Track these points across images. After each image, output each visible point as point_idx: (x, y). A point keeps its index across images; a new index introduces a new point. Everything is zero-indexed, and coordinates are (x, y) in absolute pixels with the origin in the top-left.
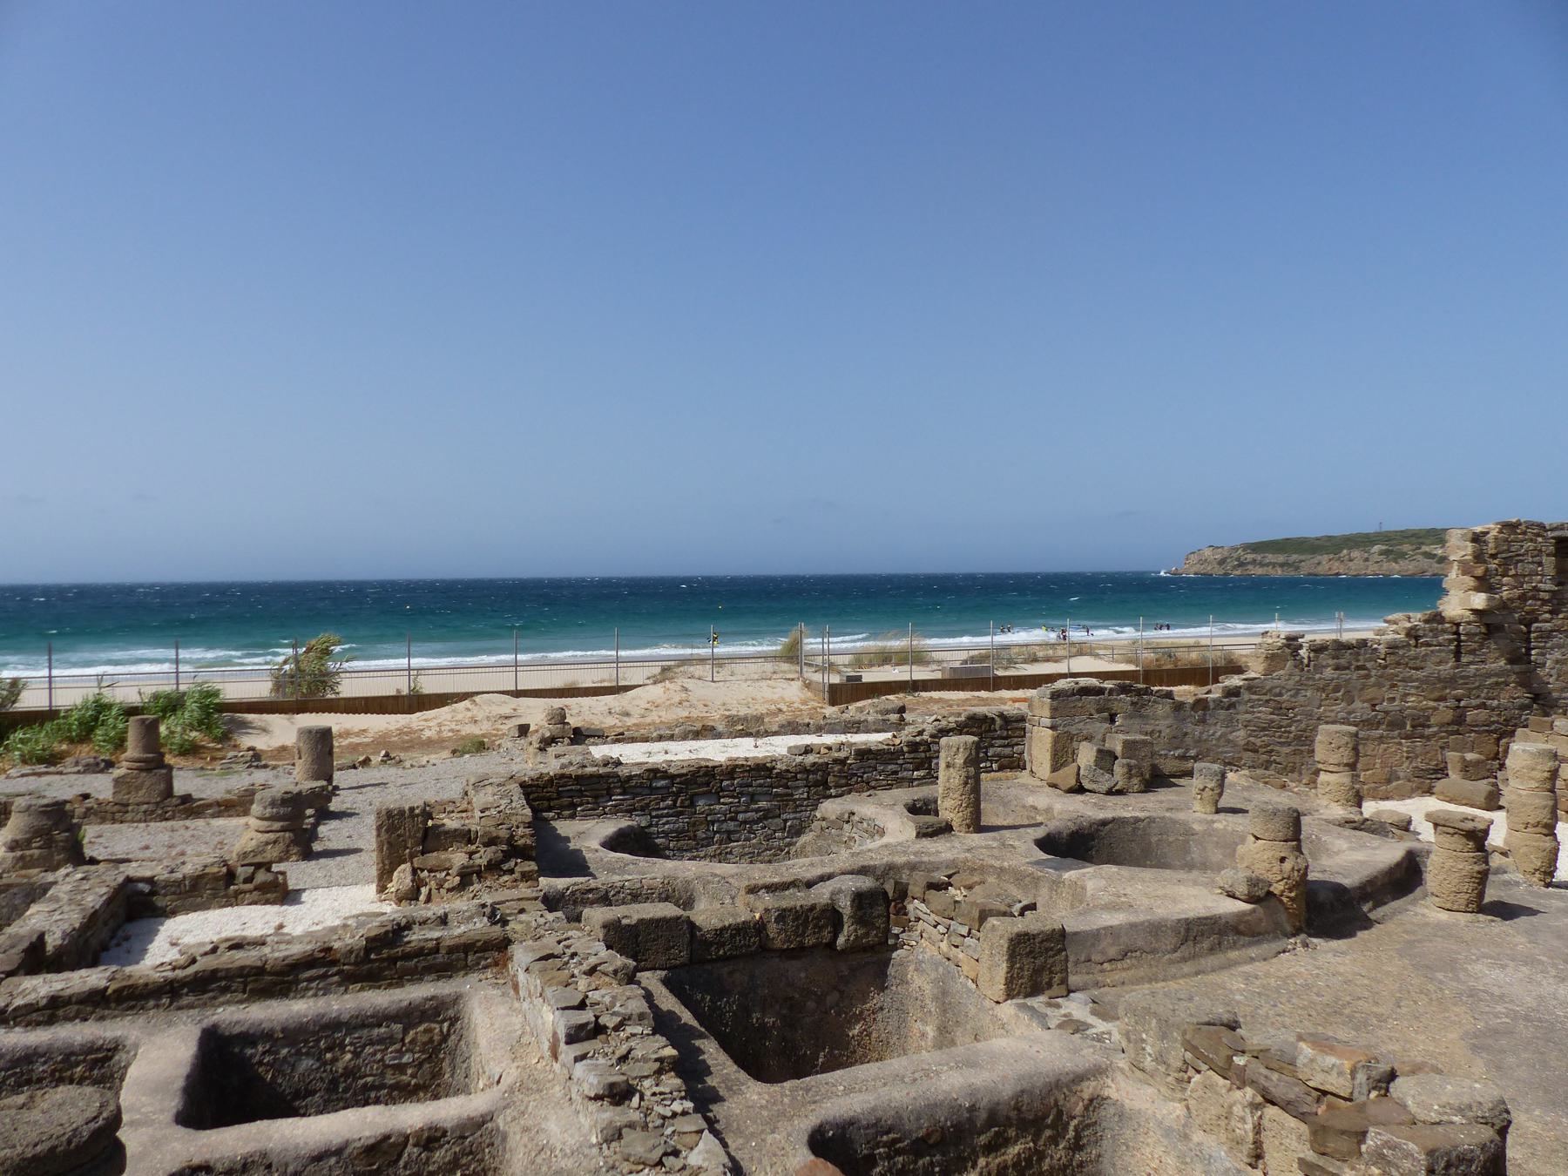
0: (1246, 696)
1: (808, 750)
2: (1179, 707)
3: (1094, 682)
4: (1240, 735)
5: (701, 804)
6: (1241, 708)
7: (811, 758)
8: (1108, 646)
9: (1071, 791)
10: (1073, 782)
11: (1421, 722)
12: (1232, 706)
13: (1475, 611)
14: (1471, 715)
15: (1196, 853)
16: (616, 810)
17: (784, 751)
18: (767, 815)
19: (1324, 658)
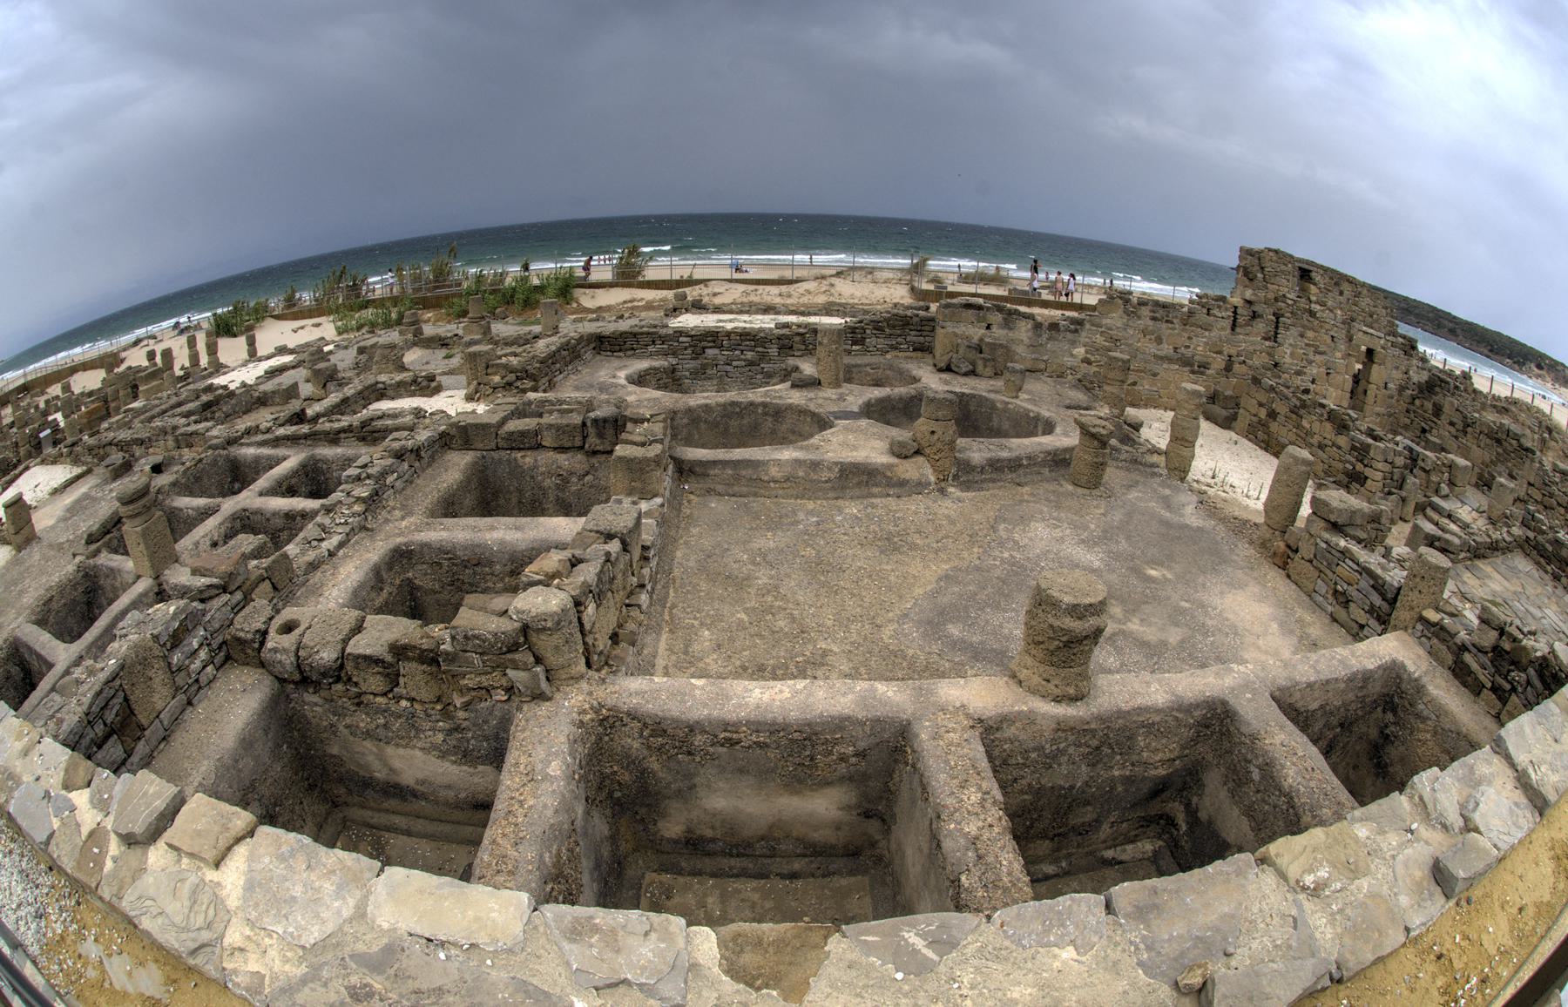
0: (1088, 326)
1: (786, 325)
2: (1038, 326)
3: (981, 301)
4: (1080, 351)
5: (710, 352)
6: (1084, 334)
7: (785, 331)
8: (878, 283)
9: (940, 370)
10: (943, 365)
11: (1204, 366)
12: (1076, 331)
13: (1249, 302)
14: (1236, 367)
15: (995, 423)
16: (657, 353)
17: (772, 326)
18: (751, 363)
19: (1145, 311)
